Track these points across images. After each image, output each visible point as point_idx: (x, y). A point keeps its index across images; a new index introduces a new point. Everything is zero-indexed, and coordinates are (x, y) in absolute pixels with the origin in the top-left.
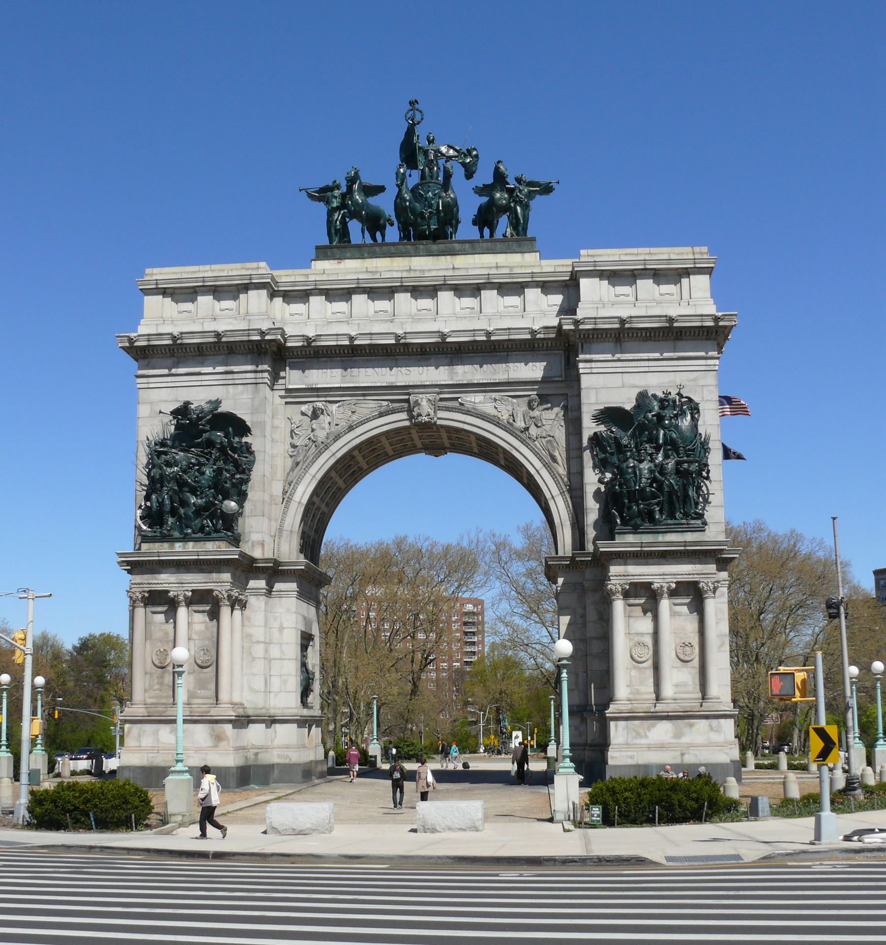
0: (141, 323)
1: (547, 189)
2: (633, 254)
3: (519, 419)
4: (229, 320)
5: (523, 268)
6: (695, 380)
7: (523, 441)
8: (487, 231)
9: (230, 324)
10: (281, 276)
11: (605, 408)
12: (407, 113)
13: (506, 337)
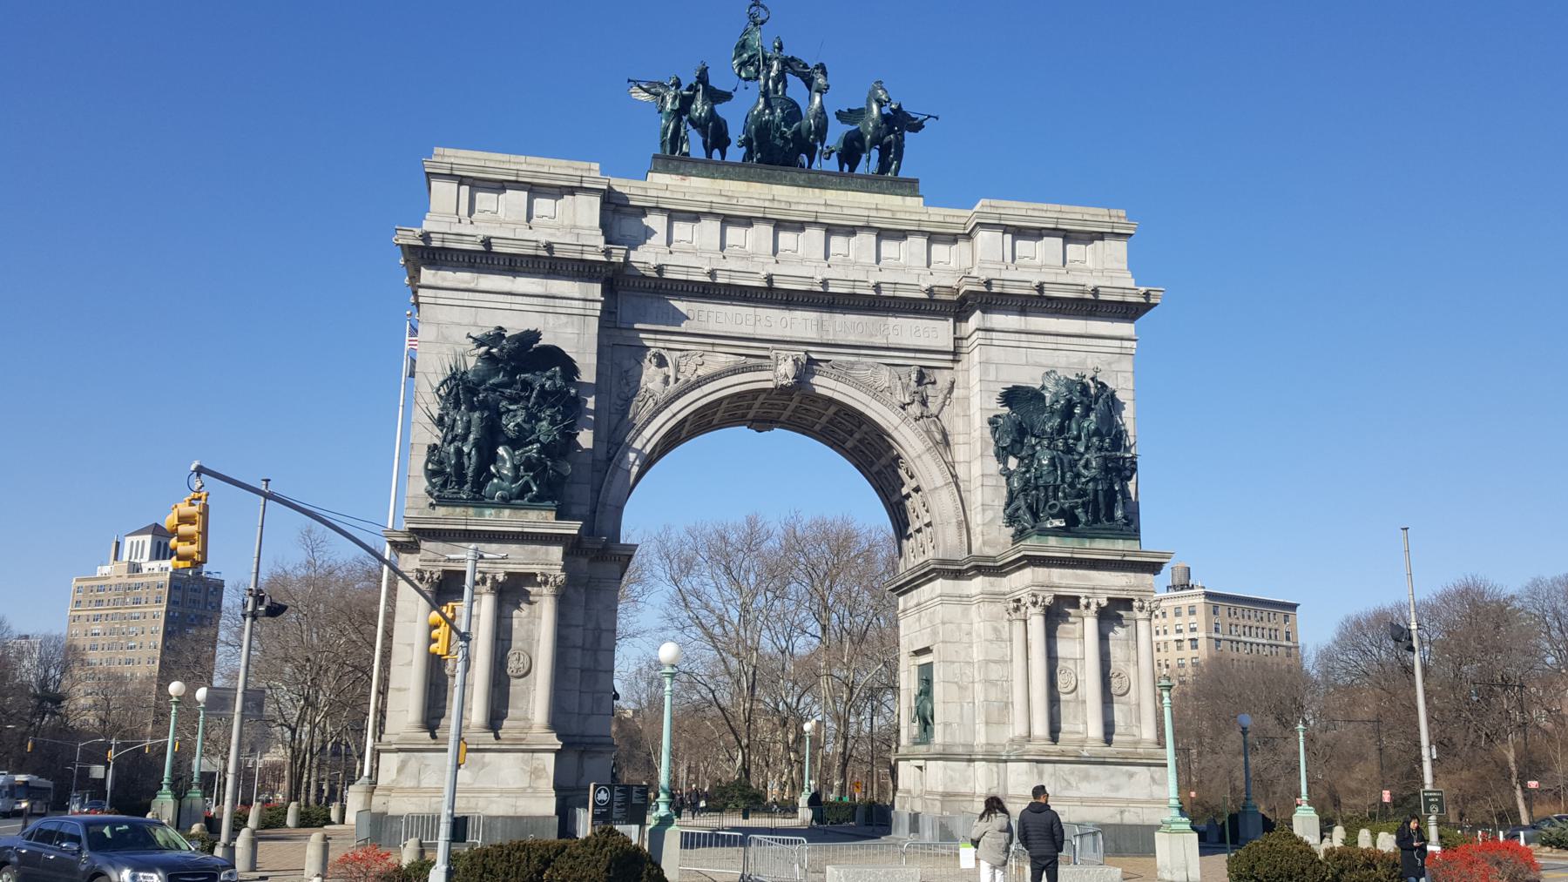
0: (427, 217)
2: (1043, 210)
3: (898, 392)
4: (553, 231)
5: (908, 214)
8: (846, 168)
11: (1014, 386)
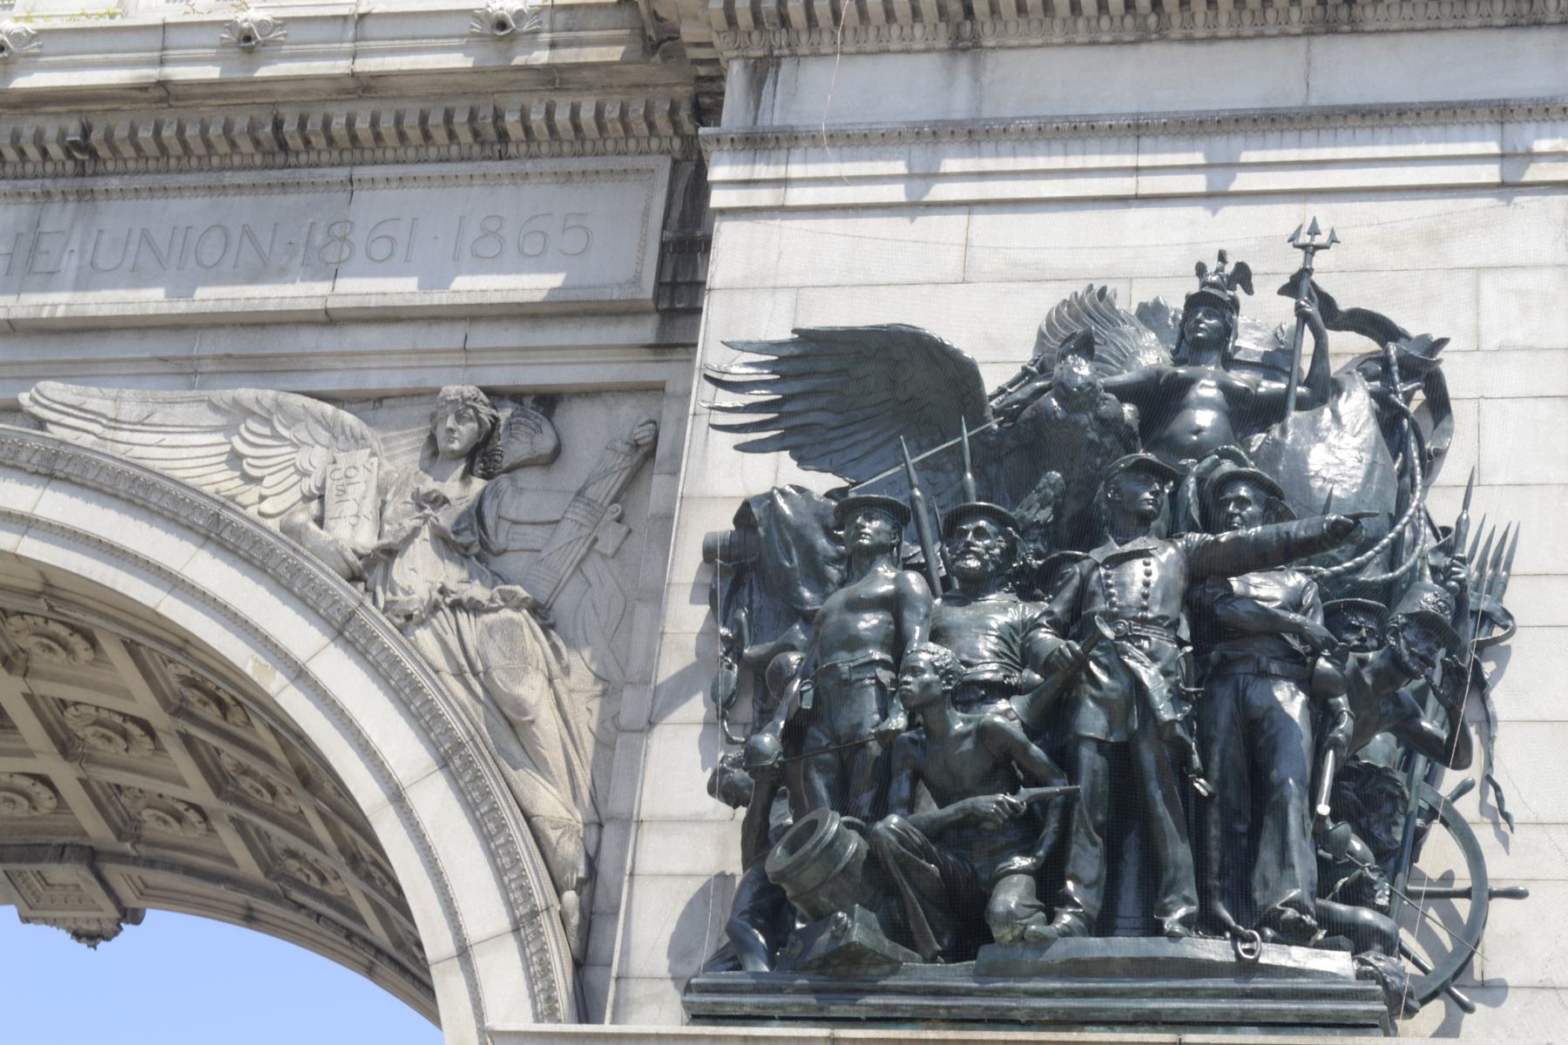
3: (349, 508)
6: (1433, 238)
13: (341, 66)
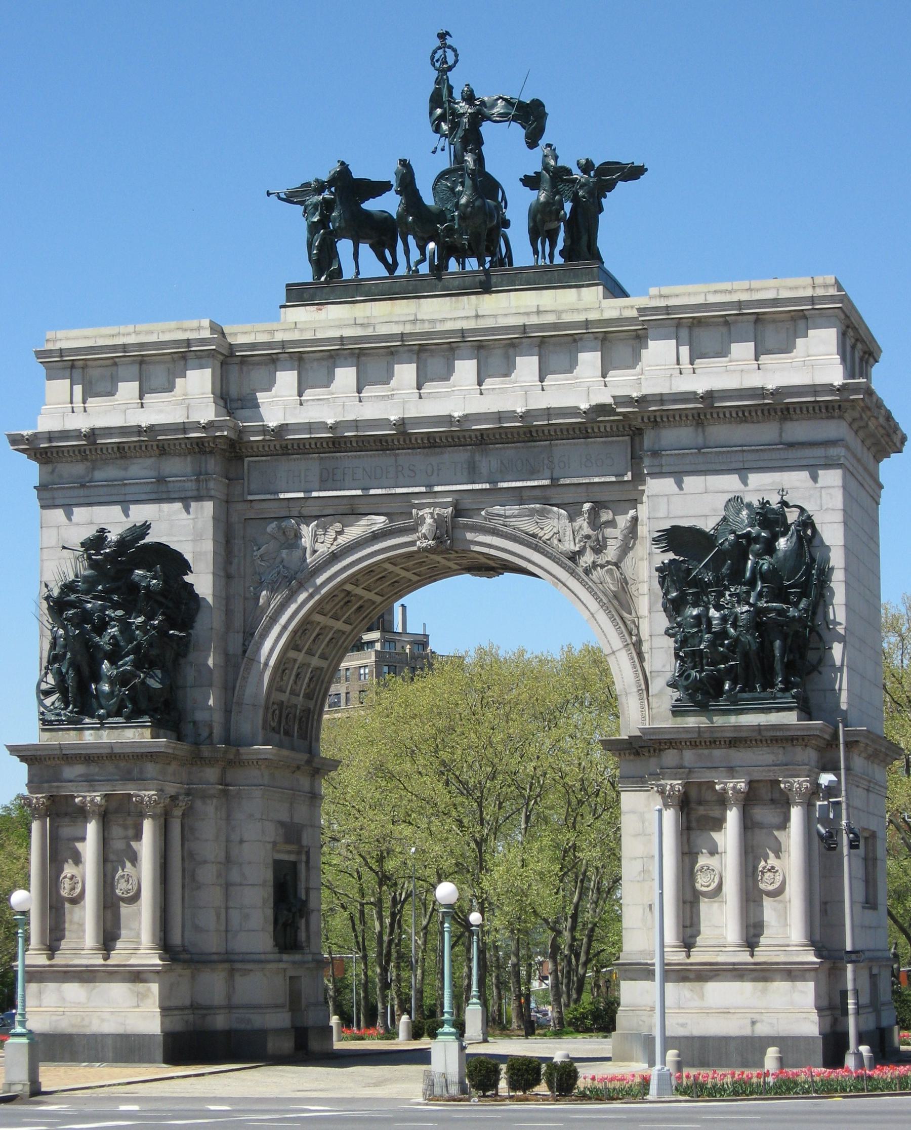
1: (634, 172)
3: (567, 538)
5: (575, 314)
7: (573, 573)
9: (161, 411)
10: (236, 334)
11: (673, 527)
12: (435, 52)
